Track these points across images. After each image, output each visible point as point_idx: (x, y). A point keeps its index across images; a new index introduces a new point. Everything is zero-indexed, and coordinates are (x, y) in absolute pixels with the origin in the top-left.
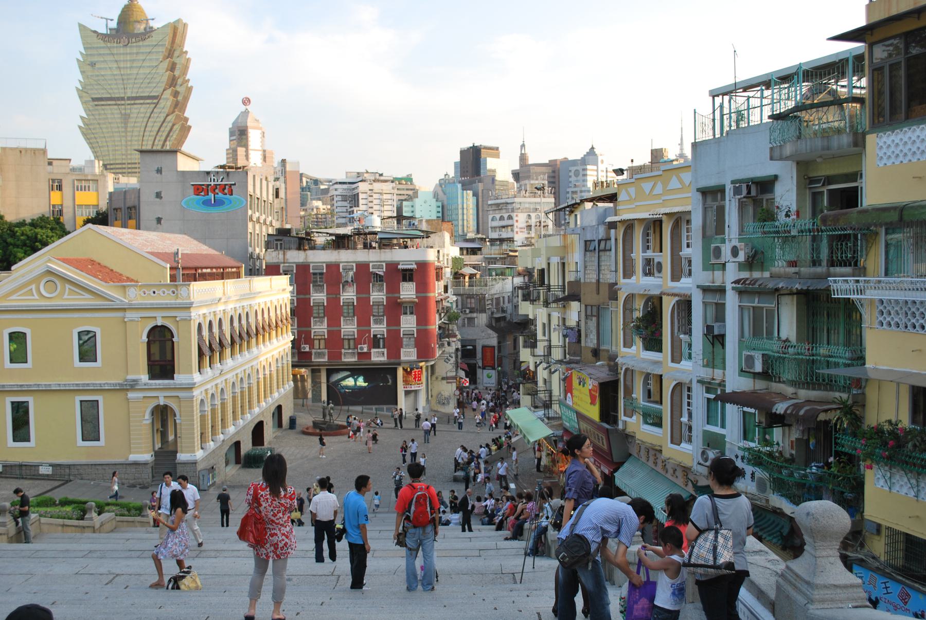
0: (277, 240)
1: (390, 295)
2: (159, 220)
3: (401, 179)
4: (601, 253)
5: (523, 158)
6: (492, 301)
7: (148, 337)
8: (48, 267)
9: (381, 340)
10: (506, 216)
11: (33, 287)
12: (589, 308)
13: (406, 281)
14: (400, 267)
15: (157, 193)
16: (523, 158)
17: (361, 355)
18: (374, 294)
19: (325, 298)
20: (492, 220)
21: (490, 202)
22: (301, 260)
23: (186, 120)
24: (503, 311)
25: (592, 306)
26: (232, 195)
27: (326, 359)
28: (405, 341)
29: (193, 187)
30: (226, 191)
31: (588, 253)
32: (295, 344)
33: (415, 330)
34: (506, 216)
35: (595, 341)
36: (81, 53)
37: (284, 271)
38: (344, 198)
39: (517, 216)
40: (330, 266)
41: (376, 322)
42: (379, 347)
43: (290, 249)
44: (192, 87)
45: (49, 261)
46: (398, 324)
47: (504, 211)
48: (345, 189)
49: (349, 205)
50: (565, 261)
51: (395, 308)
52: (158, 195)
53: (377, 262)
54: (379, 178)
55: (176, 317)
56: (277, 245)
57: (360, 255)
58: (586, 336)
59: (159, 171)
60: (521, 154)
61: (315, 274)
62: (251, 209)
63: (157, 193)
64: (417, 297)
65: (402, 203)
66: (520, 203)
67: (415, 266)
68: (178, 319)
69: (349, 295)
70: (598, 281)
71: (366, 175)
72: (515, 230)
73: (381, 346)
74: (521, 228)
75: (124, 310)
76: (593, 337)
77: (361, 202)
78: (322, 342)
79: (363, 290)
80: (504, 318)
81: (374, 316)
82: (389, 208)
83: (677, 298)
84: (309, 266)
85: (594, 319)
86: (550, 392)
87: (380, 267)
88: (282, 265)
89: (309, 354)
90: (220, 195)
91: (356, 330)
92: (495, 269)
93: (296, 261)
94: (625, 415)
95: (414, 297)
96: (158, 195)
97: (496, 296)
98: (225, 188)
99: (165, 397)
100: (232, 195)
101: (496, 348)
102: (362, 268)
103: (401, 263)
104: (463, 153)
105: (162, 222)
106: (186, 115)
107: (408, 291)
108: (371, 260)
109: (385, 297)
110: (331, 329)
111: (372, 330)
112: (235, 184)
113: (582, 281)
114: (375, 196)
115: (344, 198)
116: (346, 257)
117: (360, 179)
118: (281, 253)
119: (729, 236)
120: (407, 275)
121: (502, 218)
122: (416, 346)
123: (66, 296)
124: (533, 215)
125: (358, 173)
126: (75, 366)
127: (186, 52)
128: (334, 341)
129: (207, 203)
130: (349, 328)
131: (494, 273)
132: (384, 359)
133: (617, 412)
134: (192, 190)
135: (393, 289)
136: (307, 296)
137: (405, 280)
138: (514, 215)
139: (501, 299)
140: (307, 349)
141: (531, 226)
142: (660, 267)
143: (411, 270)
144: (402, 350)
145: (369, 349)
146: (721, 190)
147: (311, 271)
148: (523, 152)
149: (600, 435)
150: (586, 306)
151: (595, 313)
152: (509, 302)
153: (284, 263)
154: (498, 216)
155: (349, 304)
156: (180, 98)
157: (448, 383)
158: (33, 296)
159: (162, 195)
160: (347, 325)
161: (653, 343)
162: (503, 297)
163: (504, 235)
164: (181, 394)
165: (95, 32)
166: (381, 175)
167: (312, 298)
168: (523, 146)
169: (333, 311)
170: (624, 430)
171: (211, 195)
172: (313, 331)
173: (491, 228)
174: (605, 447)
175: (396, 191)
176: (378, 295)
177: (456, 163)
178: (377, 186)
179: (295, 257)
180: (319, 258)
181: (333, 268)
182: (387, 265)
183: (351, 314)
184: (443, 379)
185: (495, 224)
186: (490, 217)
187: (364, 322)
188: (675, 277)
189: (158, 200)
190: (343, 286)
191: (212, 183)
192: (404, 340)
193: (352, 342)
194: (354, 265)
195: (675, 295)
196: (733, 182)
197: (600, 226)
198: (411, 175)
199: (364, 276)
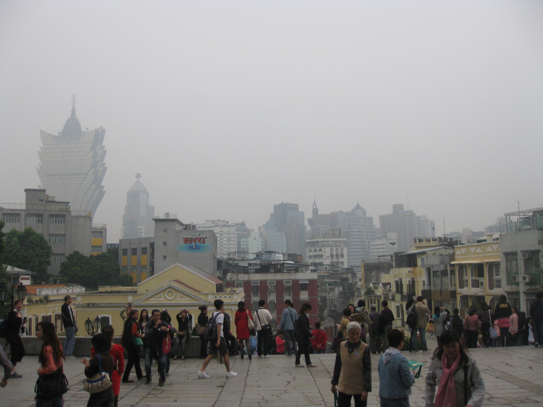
2: (165, 257)
5: (315, 211)
6: (330, 301)
10: (318, 249)
11: (162, 294)
14: (300, 282)
16: (315, 211)
18: (286, 297)
20: (309, 252)
23: (103, 187)
24: (335, 307)
26: (204, 243)
29: (183, 239)
30: (201, 241)
31: (435, 278)
34: (318, 249)
36: (41, 147)
37: (237, 285)
39: (325, 249)
43: (240, 273)
44: (107, 167)
45: (170, 281)
50: (415, 280)
52: (165, 244)
53: (287, 280)
54: (226, 225)
55: (232, 309)
56: (233, 271)
57: (279, 277)
59: (165, 231)
60: (314, 209)
61: (253, 286)
64: (309, 299)
65: (240, 240)
66: (327, 241)
67: (308, 282)
71: (219, 223)
72: (324, 257)
74: (327, 257)
79: (280, 295)
80: (335, 311)
82: (233, 243)
83: (492, 297)
84: (251, 282)
87: (289, 282)
88: (236, 282)
90: (198, 243)
91: (276, 317)
93: (244, 279)
95: (308, 298)
96: (165, 244)
97: (331, 298)
98: (201, 240)
100: (204, 243)
102: (279, 283)
103: (300, 280)
104: (275, 207)
105: (167, 258)
106: (102, 184)
108: (284, 278)
112: (206, 238)
114: (224, 235)
116: (271, 277)
117: (215, 224)
119: (520, 272)
120: (304, 287)
121: (315, 251)
123: (178, 299)
124: (334, 249)
125: (213, 221)
127: (104, 147)
129: (191, 248)
131: (327, 285)
134: (182, 241)
137: (302, 289)
138: (323, 249)
139: (334, 299)
142: (482, 284)
146: (515, 254)
147: (252, 285)
148: (315, 207)
150: (435, 301)
152: (337, 301)
153: (237, 280)
154: (313, 249)
158: (162, 298)
159: (167, 243)
162: (335, 298)
163: (317, 261)
165: (50, 135)
166: (228, 222)
167: (252, 300)
168: (315, 204)
173: (309, 256)
175: (237, 232)
178: (225, 229)
179: (243, 277)
180: (258, 277)
185: (311, 254)
186: (308, 250)
188: (491, 288)
189: (164, 246)
191: (194, 237)
194: (275, 282)
195: (490, 295)
196: (522, 252)
197: (441, 265)
198: (244, 222)
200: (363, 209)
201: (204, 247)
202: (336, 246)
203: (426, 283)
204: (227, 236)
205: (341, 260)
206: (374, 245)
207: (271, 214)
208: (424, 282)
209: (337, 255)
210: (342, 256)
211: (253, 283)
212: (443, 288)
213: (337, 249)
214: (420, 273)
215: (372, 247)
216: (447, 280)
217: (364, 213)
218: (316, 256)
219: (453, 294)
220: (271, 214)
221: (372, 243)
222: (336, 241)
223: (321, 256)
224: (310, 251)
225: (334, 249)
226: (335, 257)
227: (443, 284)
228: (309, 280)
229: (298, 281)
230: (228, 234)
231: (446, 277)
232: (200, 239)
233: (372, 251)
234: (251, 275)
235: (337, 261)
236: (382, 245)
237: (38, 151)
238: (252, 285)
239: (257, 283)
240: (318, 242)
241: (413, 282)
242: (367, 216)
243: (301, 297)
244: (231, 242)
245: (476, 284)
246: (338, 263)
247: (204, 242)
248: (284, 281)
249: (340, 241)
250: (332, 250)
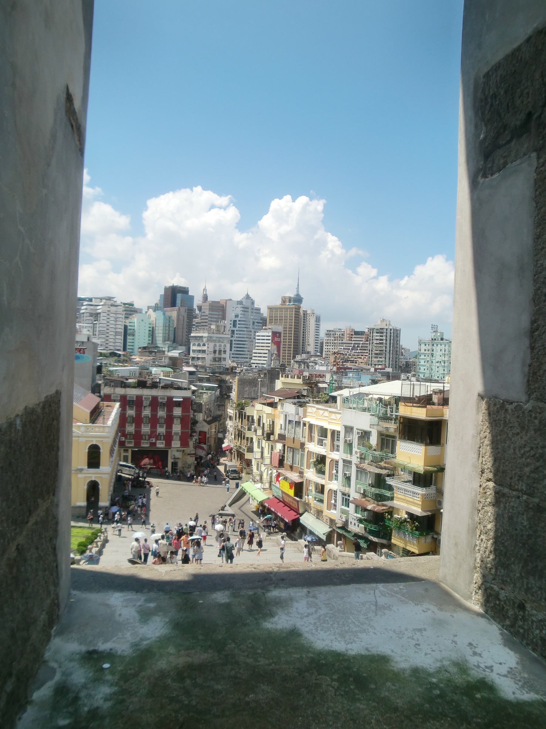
0: (111, 382)
5: (205, 298)
12: (289, 449)
13: (176, 406)
14: (174, 399)
16: (205, 298)
19: (134, 413)
21: (192, 335)
25: (291, 448)
26: (84, 354)
27: (132, 445)
28: (175, 437)
30: (81, 352)
33: (180, 431)
38: (91, 315)
41: (160, 427)
43: (117, 387)
47: (201, 341)
48: (91, 309)
49: (94, 319)
56: (110, 384)
58: (287, 459)
67: (182, 400)
69: (147, 412)
70: (294, 438)
73: (162, 439)
75: (79, 437)
76: (290, 460)
77: (102, 318)
81: (159, 424)
85: (291, 453)
89: (124, 442)
92: (205, 387)
101: (207, 433)
102: (155, 399)
104: (166, 289)
109: (165, 414)
110: (137, 429)
111: (158, 431)
113: (287, 436)
114: (112, 315)
115: (91, 315)
116: (146, 393)
118: (113, 388)
120: (178, 404)
128: (138, 436)
130: (146, 429)
131: (205, 389)
135: (170, 410)
140: (124, 440)
141: (216, 351)
144: (173, 442)
145: (156, 441)
146: (352, 429)
147: (128, 399)
148: (205, 293)
150: (288, 447)
154: (197, 344)
155: (146, 417)
157: (191, 457)
160: (145, 428)
161: (321, 472)
169: (138, 420)
172: (127, 430)
174: (296, 507)
175: (124, 313)
176: (162, 413)
177: (161, 295)
178: (113, 309)
179: (120, 391)
180: (133, 392)
181: (139, 399)
182: (167, 398)
183: (148, 422)
184: (188, 454)
187: (154, 427)
194: (151, 397)
196: (357, 429)
199: (154, 403)
200: (252, 299)
202: (219, 341)
203: (283, 427)
204: (115, 316)
205: (223, 356)
206: (259, 336)
207: (161, 295)
208: (281, 425)
209: (220, 351)
210: (225, 352)
211: (130, 397)
213: (220, 346)
215: (257, 338)
216: (299, 430)
217: (253, 303)
218: (199, 351)
219: (303, 445)
220: (161, 295)
221: (257, 334)
222: (220, 337)
223: (204, 351)
224: (194, 345)
225: (218, 344)
226: (217, 352)
228: (183, 398)
229: (172, 398)
230: (116, 314)
233: (257, 341)
234: (128, 389)
235: (220, 356)
236: (267, 336)
238: (128, 399)
239: (133, 397)
241: (273, 422)
242: (256, 306)
244: (118, 323)
245: (321, 443)
246: (220, 359)
247: (84, 353)
249: (223, 338)
250: (215, 346)
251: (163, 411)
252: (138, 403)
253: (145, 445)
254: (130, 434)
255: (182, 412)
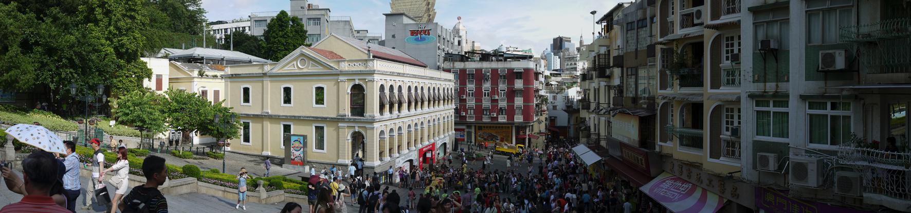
0: (450, 56)
1: (509, 86)
3: (527, 51)
4: (639, 30)
7: (351, 91)
8: (301, 51)
9: (504, 111)
15: (393, 35)
16: (581, 42)
17: (493, 118)
22: (462, 67)
28: (517, 111)
29: (410, 32)
30: (426, 33)
32: (457, 111)
34: (573, 63)
35: (634, 93)
40: (477, 70)
42: (502, 114)
43: (456, 61)
46: (513, 102)
51: (511, 94)
52: (394, 36)
56: (450, 59)
57: (494, 65)
58: (627, 89)
61: (469, 74)
62: (439, 43)
63: (393, 35)
64: (524, 88)
68: (367, 80)
73: (504, 113)
75: (338, 75)
78: (472, 111)
79: (495, 83)
86: (599, 134)
94: (660, 141)
96: (394, 36)
99: (358, 127)
102: (494, 71)
104: (555, 40)
107: (519, 84)
116: (485, 65)
118: (452, 63)
120: (519, 75)
121: (571, 64)
122: (523, 114)
126: (313, 106)
129: (417, 40)
132: (505, 121)
133: (654, 139)
136: (465, 86)
140: (464, 114)
143: (521, 73)
144: (515, 116)
145: (497, 115)
149: (639, 158)
150: (627, 68)
151: (634, 73)
154: (569, 63)
156: (431, 17)
164: (368, 126)
168: (581, 37)
170: (660, 152)
171: (419, 36)
172: (467, 105)
177: (551, 45)
179: (459, 65)
180: (471, 66)
181: (479, 71)
185: (568, 67)
186: (566, 64)
189: (393, 38)
190: (484, 81)
191: (420, 29)
192: (517, 111)
193: (488, 111)
201: (429, 39)
212: (639, 46)
214: (616, 38)
224: (567, 65)
227: (640, 40)
231: (644, 29)
232: (425, 32)
234: (467, 63)
237: (390, 3)
240: (574, 57)
243: (515, 85)
248: (499, 70)
251: (504, 83)
252: (479, 76)
253: (486, 120)
254: (471, 108)
255: (524, 85)
